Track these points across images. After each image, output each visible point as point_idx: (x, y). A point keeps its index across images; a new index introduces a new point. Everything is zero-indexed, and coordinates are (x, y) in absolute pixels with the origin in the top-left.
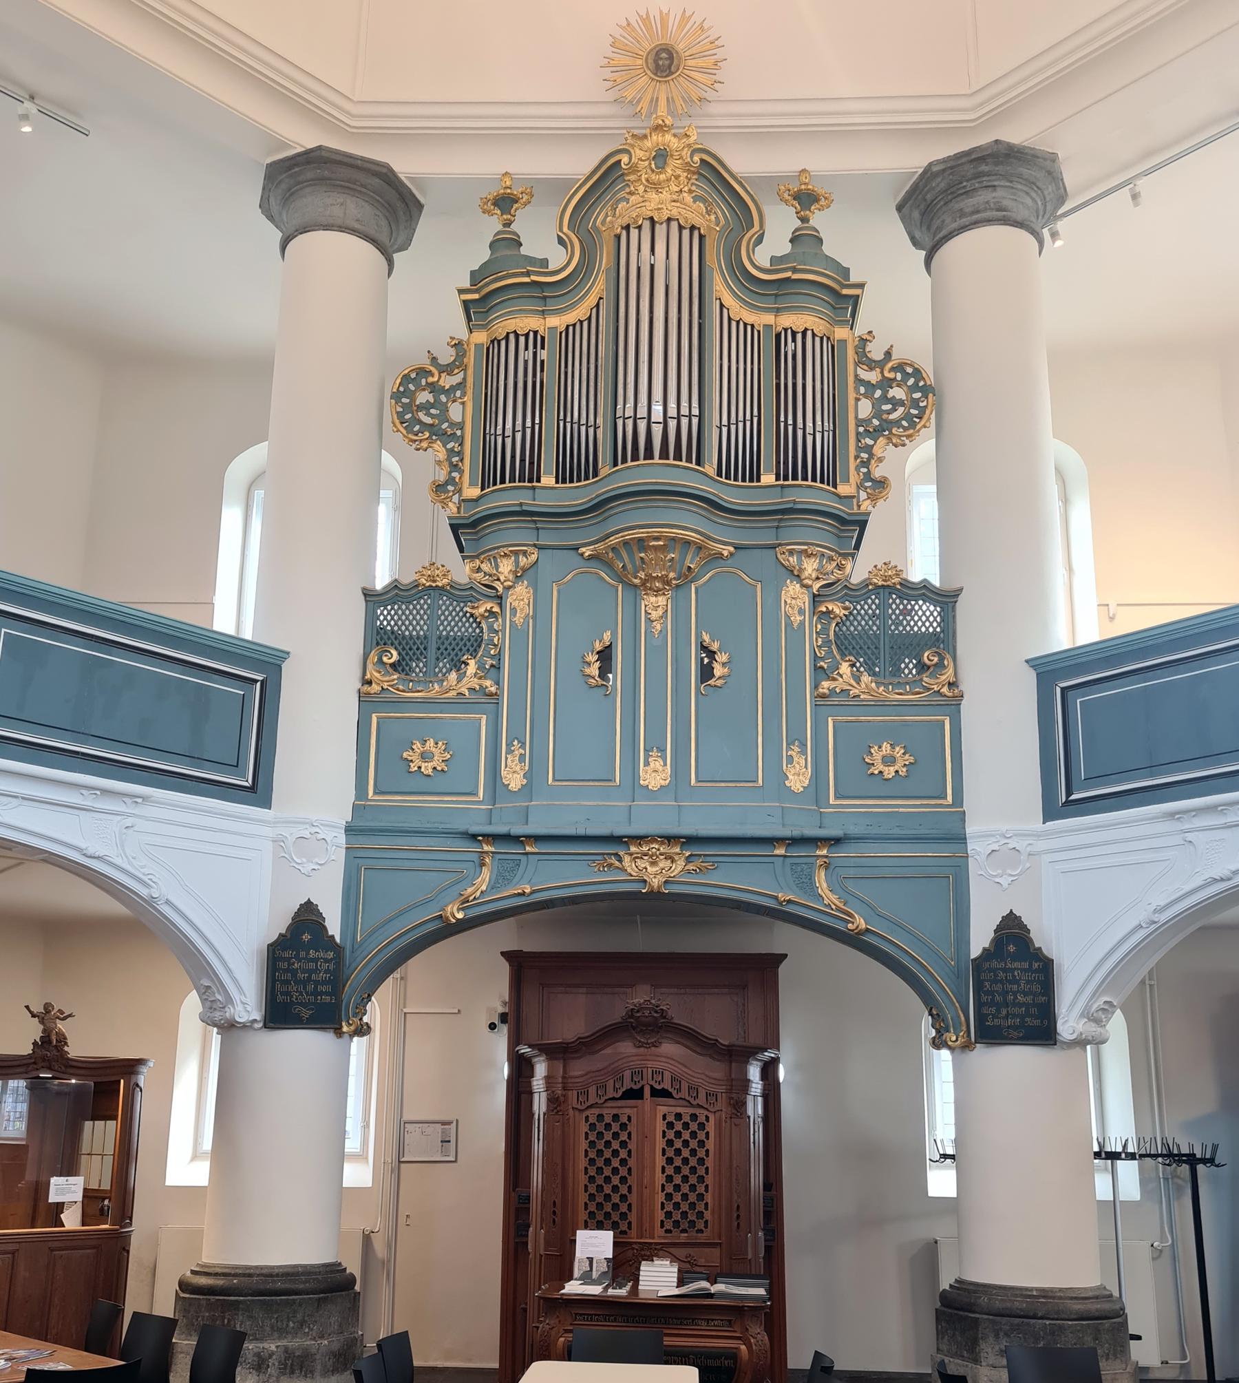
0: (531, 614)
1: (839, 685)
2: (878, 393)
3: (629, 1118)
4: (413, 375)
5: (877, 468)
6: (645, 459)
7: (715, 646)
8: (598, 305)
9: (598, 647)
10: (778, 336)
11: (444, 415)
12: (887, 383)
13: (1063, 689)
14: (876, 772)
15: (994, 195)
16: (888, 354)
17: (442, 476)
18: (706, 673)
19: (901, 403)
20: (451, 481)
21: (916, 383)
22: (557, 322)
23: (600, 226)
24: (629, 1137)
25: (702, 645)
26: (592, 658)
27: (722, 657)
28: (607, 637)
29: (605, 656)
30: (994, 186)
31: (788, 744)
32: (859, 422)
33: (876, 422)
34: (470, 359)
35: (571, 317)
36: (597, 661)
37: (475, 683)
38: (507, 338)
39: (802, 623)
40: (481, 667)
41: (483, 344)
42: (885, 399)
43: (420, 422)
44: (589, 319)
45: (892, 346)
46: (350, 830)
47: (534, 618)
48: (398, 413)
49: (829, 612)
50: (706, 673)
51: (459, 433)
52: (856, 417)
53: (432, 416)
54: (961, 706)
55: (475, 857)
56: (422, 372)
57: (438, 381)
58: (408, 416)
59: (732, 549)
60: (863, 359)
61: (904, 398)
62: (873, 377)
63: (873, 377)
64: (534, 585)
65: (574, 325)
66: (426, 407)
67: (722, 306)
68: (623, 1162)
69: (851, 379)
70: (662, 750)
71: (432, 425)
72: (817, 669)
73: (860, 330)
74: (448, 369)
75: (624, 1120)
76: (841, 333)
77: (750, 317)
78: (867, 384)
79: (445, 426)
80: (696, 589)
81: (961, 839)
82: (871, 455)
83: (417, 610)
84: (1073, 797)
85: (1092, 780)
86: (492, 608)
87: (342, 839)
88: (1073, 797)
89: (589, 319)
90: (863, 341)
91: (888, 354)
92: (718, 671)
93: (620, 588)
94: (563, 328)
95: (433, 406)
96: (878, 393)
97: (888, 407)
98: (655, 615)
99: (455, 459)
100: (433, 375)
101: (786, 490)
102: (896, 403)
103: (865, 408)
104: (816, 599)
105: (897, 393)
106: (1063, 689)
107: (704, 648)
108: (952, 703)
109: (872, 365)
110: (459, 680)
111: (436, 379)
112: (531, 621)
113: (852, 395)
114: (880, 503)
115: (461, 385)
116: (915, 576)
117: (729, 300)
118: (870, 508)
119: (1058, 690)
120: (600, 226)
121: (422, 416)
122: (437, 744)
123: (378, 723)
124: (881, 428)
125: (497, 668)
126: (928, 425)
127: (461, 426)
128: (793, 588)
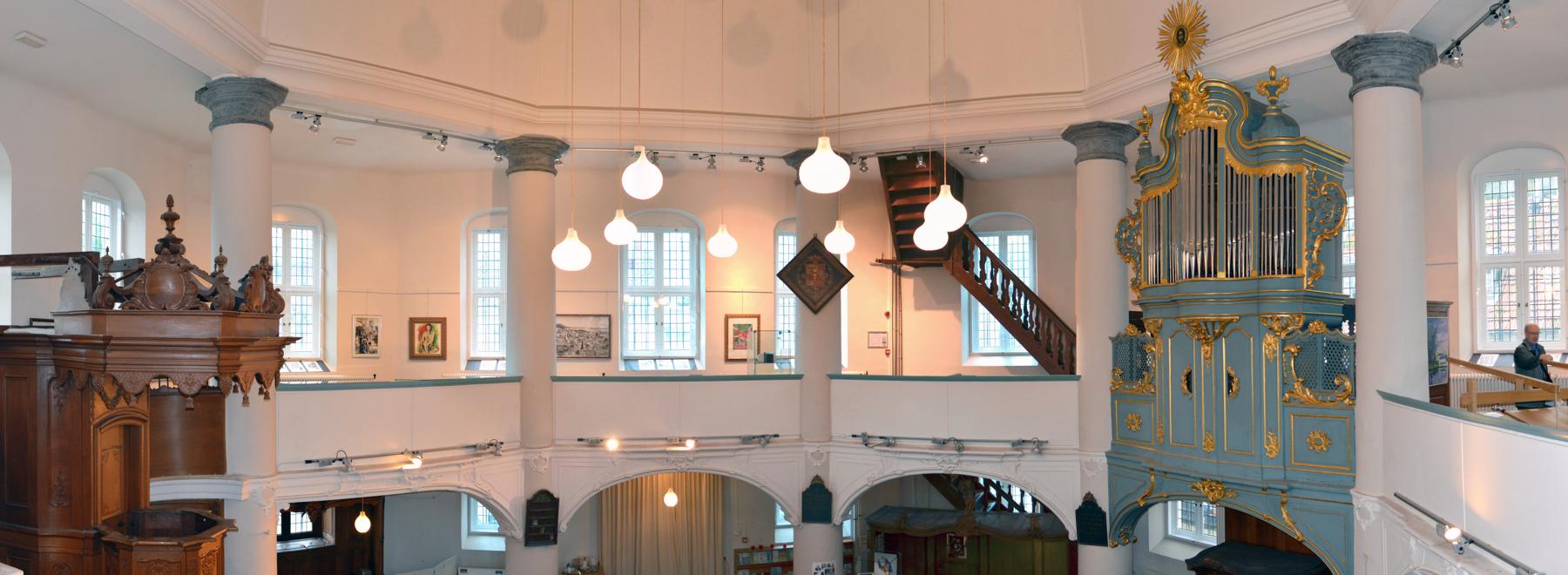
7: (1233, 373)
9: (1185, 372)
10: (1261, 180)
15: (1370, 65)
18: (1230, 387)
26: (1183, 378)
27: (1236, 380)
30: (1369, 60)
31: (1267, 432)
39: (1275, 358)
46: (1108, 455)
49: (1289, 350)
67: (1232, 169)
72: (1284, 384)
87: (1105, 460)
101: (1261, 281)
104: (1284, 343)
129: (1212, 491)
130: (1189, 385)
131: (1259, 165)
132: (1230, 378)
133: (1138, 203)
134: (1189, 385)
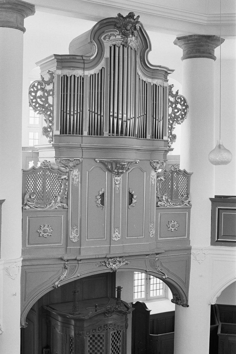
0: (80, 181)
1: (162, 203)
2: (174, 106)
3: (103, 335)
4: (36, 84)
5: (173, 131)
6: (125, 136)
7: (133, 193)
8: (101, 70)
9: (101, 193)
11: (47, 101)
12: (176, 102)
13: (219, 209)
14: (170, 230)
16: (177, 93)
17: (46, 125)
18: (131, 202)
19: (180, 110)
20: (50, 127)
21: (184, 104)
22: (88, 73)
23: (103, 39)
24: (103, 341)
25: (129, 192)
27: (135, 197)
28: (103, 190)
29: (102, 196)
32: (169, 115)
33: (173, 115)
34: (55, 80)
35: (92, 72)
36: (100, 198)
37: (60, 205)
38: (71, 77)
40: (62, 198)
41: (60, 75)
42: (176, 107)
43: (39, 104)
44: (98, 74)
45: (178, 90)
47: (81, 183)
48: (31, 99)
50: (131, 202)
51: (51, 108)
52: (168, 114)
53: (42, 101)
54: (191, 209)
55: (63, 265)
56: (39, 83)
57: (45, 88)
58: (34, 101)
59: (139, 161)
60: (171, 93)
61: (181, 108)
62: (172, 99)
63: (172, 99)
64: (81, 171)
65: (93, 75)
66: (40, 97)
68: (101, 348)
69: (168, 100)
70: (118, 228)
71: (43, 105)
73: (170, 83)
74: (48, 83)
75: (102, 336)
76: (166, 84)
77: (145, 79)
78: (171, 102)
79: (47, 105)
80: (128, 173)
81: (190, 249)
82: (172, 127)
83: (54, 190)
84: (218, 240)
85: (225, 236)
86: (66, 178)
88: (218, 240)
89: (98, 74)
90: (171, 87)
91: (177, 93)
92: (134, 201)
93: (107, 173)
94: (89, 76)
95: (43, 97)
96: (174, 106)
97: (176, 111)
98: (117, 183)
99: (50, 119)
100: (43, 86)
102: (179, 110)
103: (170, 110)
105: (179, 106)
106: (219, 209)
107: (130, 193)
108: (188, 208)
109: (173, 96)
110: (56, 202)
111: (43, 87)
112: (79, 184)
113: (168, 106)
114: (174, 143)
115: (53, 90)
116: (182, 168)
117: (140, 73)
118: (171, 145)
119: (217, 209)
120: (103, 39)
121: (39, 100)
122: (49, 226)
123: (29, 219)
124: (175, 119)
125: (67, 198)
126: (186, 118)
127: (53, 106)
128: (153, 174)
129: (114, 264)
130: (102, 202)
131: (153, 78)
132: (131, 196)
133: (51, 74)
134: (102, 202)
